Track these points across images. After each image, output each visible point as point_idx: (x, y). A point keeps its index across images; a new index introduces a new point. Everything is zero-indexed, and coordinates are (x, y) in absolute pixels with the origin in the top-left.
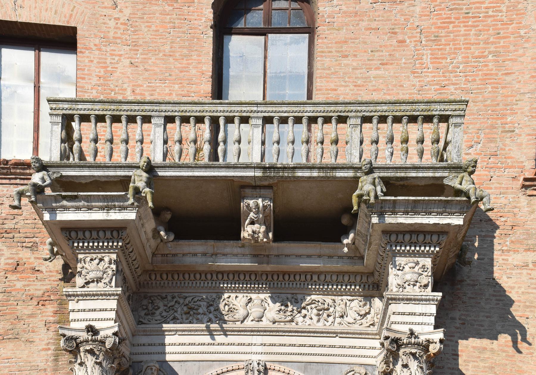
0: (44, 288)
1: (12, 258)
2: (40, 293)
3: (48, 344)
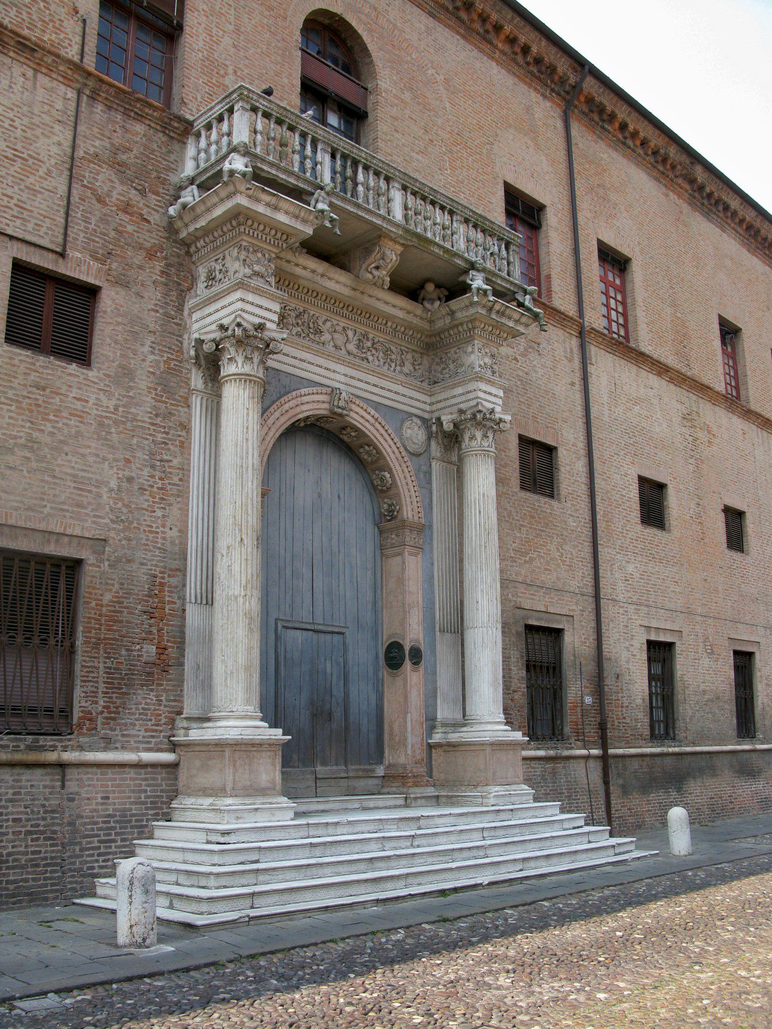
0: (153, 241)
1: (124, 196)
2: (148, 245)
3: (156, 305)
